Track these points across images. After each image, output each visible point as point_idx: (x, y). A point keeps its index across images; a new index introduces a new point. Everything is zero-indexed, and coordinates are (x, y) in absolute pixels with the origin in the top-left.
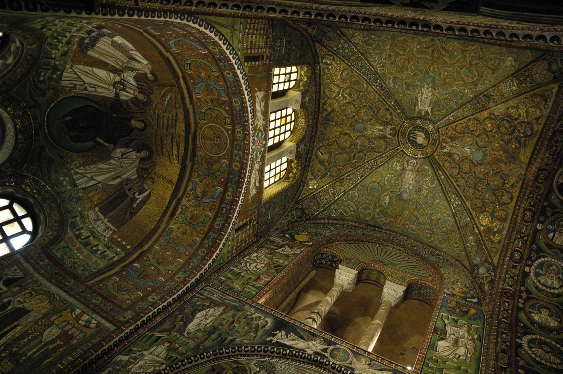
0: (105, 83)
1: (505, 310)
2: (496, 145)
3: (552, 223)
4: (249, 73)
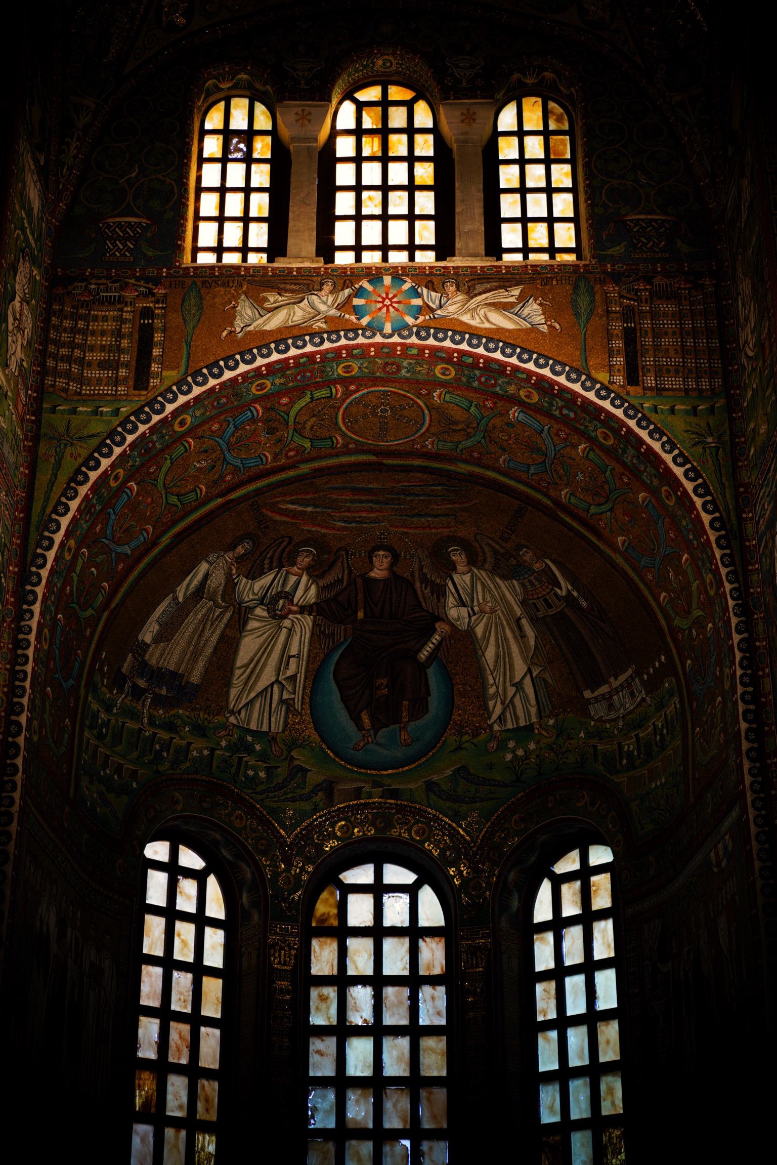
0: (274, 637)
4: (178, 367)
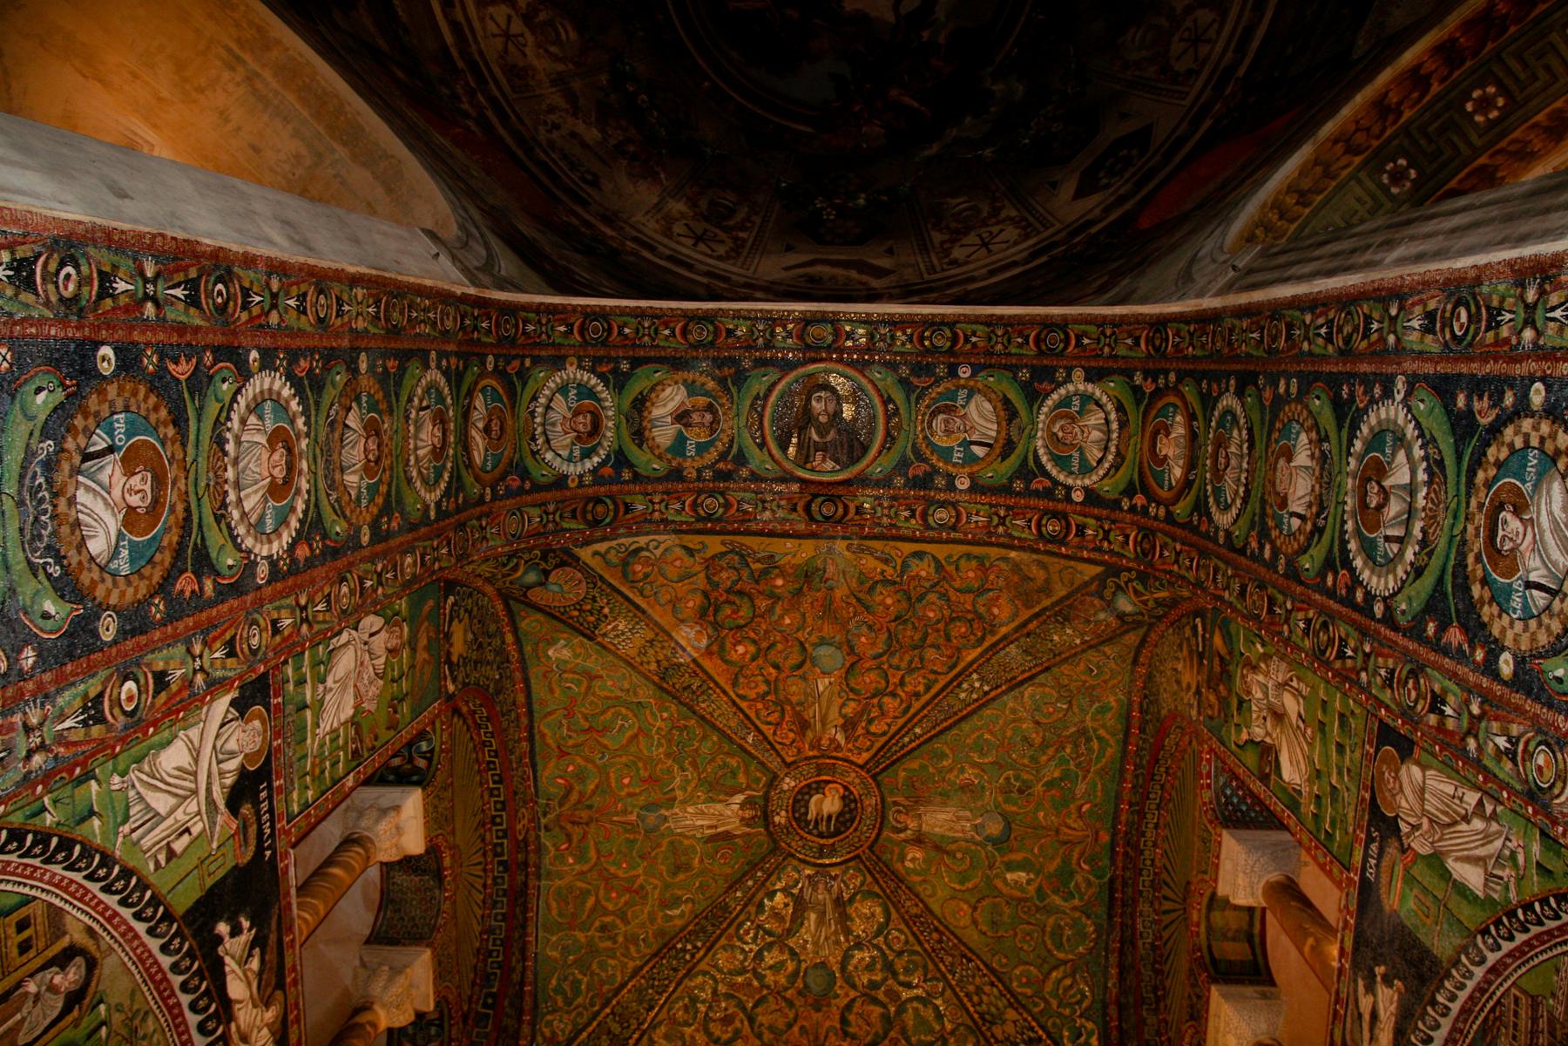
1: (1177, 561)
2: (787, 621)
3: (946, 454)
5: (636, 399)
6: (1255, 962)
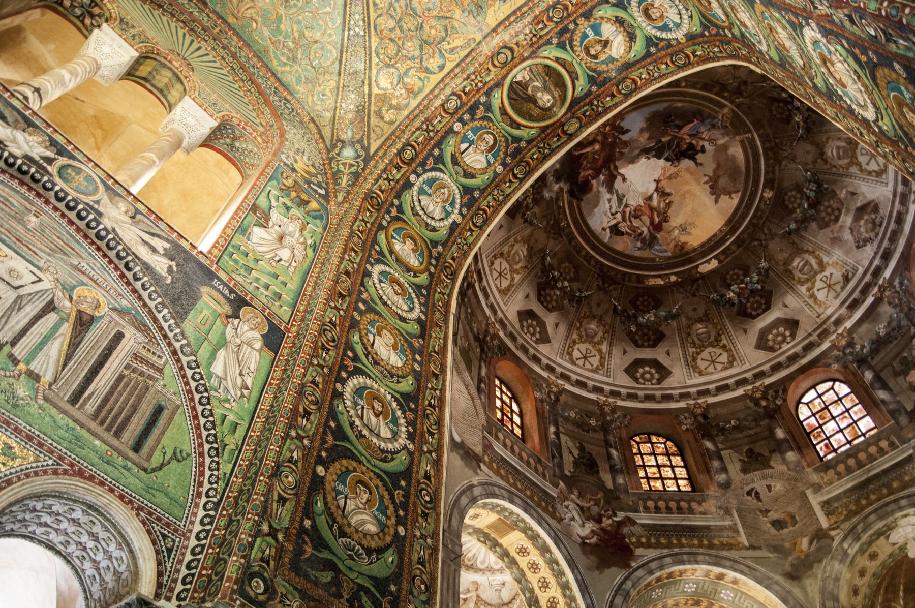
1: (363, 220)
3: (475, 131)
5: (636, 38)
6: (133, 76)
